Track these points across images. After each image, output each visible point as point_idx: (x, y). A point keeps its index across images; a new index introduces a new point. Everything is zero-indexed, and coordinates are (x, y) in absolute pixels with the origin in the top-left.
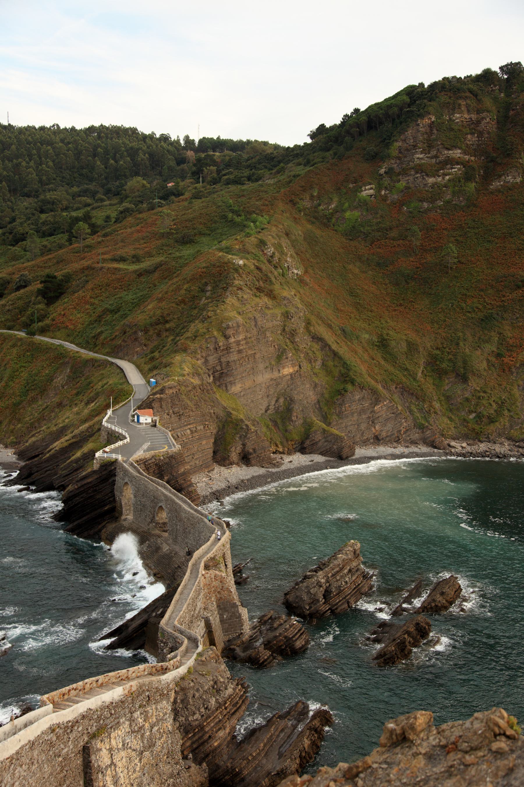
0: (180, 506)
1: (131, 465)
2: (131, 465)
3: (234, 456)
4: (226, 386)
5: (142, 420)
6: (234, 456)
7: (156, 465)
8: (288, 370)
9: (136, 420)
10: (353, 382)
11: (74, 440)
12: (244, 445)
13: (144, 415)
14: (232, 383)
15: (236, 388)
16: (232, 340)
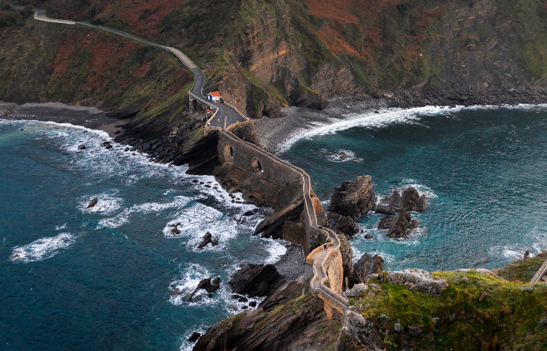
0: (272, 160)
1: (228, 133)
2: (228, 133)
3: (260, 113)
4: (248, 67)
5: (214, 99)
6: (260, 113)
7: (238, 131)
8: (282, 52)
9: (209, 98)
10: (323, 58)
11: (164, 111)
12: (265, 107)
13: (214, 96)
14: (251, 64)
15: (253, 68)
16: (250, 36)
